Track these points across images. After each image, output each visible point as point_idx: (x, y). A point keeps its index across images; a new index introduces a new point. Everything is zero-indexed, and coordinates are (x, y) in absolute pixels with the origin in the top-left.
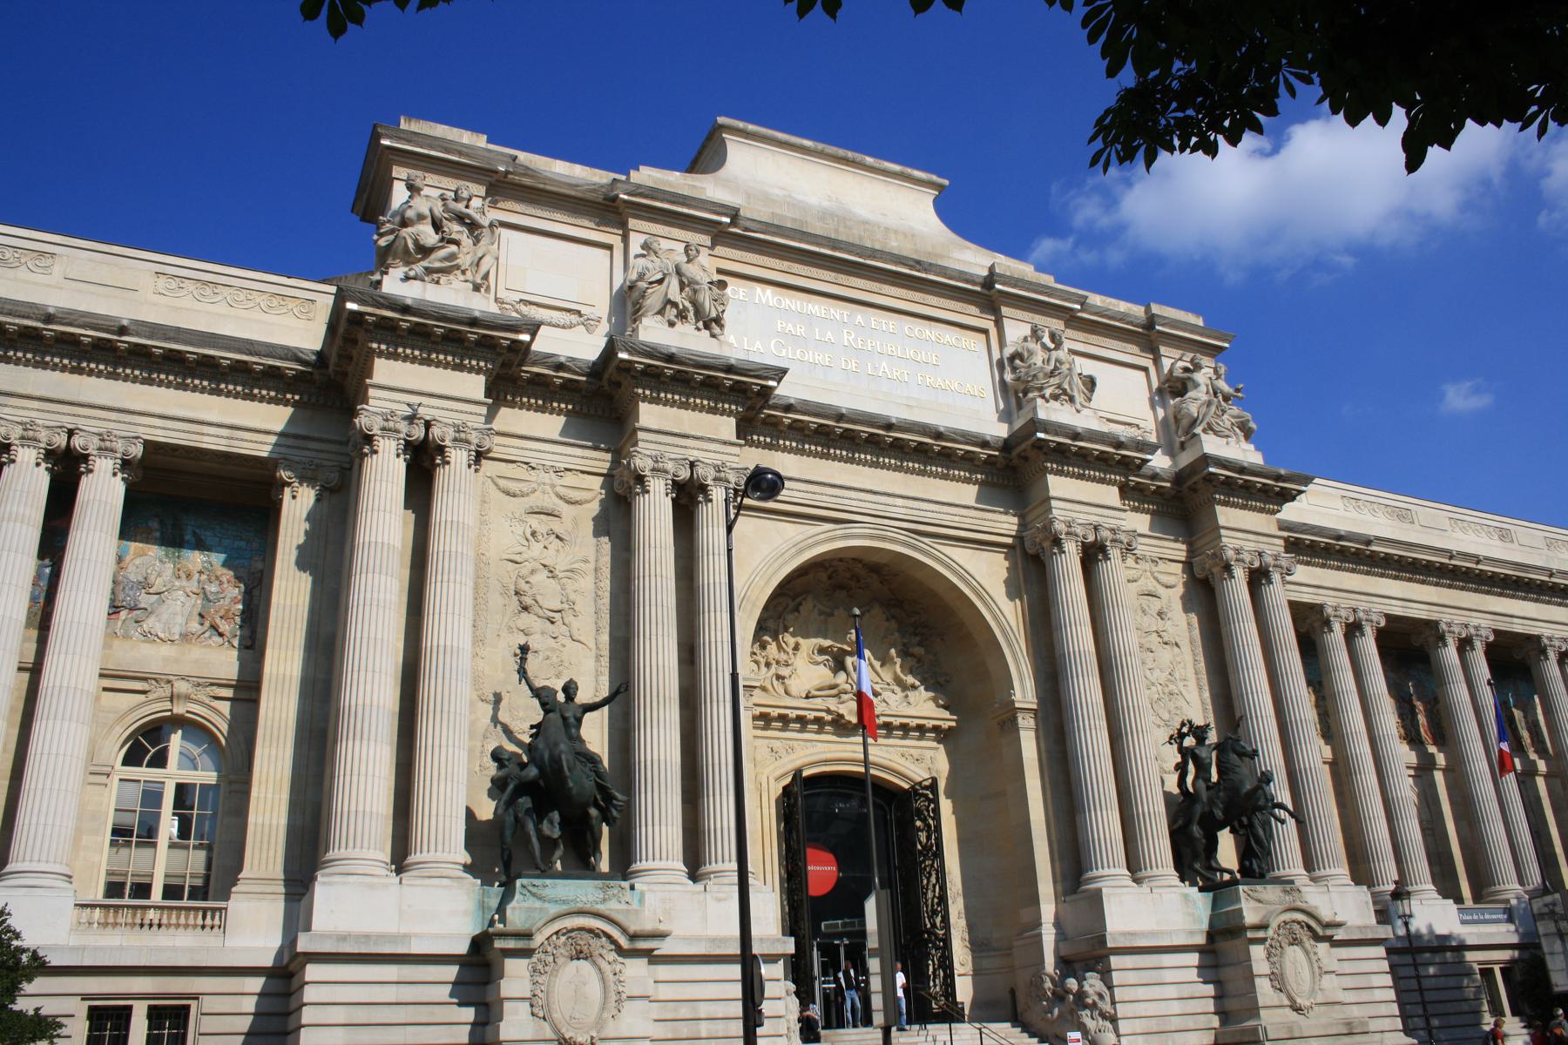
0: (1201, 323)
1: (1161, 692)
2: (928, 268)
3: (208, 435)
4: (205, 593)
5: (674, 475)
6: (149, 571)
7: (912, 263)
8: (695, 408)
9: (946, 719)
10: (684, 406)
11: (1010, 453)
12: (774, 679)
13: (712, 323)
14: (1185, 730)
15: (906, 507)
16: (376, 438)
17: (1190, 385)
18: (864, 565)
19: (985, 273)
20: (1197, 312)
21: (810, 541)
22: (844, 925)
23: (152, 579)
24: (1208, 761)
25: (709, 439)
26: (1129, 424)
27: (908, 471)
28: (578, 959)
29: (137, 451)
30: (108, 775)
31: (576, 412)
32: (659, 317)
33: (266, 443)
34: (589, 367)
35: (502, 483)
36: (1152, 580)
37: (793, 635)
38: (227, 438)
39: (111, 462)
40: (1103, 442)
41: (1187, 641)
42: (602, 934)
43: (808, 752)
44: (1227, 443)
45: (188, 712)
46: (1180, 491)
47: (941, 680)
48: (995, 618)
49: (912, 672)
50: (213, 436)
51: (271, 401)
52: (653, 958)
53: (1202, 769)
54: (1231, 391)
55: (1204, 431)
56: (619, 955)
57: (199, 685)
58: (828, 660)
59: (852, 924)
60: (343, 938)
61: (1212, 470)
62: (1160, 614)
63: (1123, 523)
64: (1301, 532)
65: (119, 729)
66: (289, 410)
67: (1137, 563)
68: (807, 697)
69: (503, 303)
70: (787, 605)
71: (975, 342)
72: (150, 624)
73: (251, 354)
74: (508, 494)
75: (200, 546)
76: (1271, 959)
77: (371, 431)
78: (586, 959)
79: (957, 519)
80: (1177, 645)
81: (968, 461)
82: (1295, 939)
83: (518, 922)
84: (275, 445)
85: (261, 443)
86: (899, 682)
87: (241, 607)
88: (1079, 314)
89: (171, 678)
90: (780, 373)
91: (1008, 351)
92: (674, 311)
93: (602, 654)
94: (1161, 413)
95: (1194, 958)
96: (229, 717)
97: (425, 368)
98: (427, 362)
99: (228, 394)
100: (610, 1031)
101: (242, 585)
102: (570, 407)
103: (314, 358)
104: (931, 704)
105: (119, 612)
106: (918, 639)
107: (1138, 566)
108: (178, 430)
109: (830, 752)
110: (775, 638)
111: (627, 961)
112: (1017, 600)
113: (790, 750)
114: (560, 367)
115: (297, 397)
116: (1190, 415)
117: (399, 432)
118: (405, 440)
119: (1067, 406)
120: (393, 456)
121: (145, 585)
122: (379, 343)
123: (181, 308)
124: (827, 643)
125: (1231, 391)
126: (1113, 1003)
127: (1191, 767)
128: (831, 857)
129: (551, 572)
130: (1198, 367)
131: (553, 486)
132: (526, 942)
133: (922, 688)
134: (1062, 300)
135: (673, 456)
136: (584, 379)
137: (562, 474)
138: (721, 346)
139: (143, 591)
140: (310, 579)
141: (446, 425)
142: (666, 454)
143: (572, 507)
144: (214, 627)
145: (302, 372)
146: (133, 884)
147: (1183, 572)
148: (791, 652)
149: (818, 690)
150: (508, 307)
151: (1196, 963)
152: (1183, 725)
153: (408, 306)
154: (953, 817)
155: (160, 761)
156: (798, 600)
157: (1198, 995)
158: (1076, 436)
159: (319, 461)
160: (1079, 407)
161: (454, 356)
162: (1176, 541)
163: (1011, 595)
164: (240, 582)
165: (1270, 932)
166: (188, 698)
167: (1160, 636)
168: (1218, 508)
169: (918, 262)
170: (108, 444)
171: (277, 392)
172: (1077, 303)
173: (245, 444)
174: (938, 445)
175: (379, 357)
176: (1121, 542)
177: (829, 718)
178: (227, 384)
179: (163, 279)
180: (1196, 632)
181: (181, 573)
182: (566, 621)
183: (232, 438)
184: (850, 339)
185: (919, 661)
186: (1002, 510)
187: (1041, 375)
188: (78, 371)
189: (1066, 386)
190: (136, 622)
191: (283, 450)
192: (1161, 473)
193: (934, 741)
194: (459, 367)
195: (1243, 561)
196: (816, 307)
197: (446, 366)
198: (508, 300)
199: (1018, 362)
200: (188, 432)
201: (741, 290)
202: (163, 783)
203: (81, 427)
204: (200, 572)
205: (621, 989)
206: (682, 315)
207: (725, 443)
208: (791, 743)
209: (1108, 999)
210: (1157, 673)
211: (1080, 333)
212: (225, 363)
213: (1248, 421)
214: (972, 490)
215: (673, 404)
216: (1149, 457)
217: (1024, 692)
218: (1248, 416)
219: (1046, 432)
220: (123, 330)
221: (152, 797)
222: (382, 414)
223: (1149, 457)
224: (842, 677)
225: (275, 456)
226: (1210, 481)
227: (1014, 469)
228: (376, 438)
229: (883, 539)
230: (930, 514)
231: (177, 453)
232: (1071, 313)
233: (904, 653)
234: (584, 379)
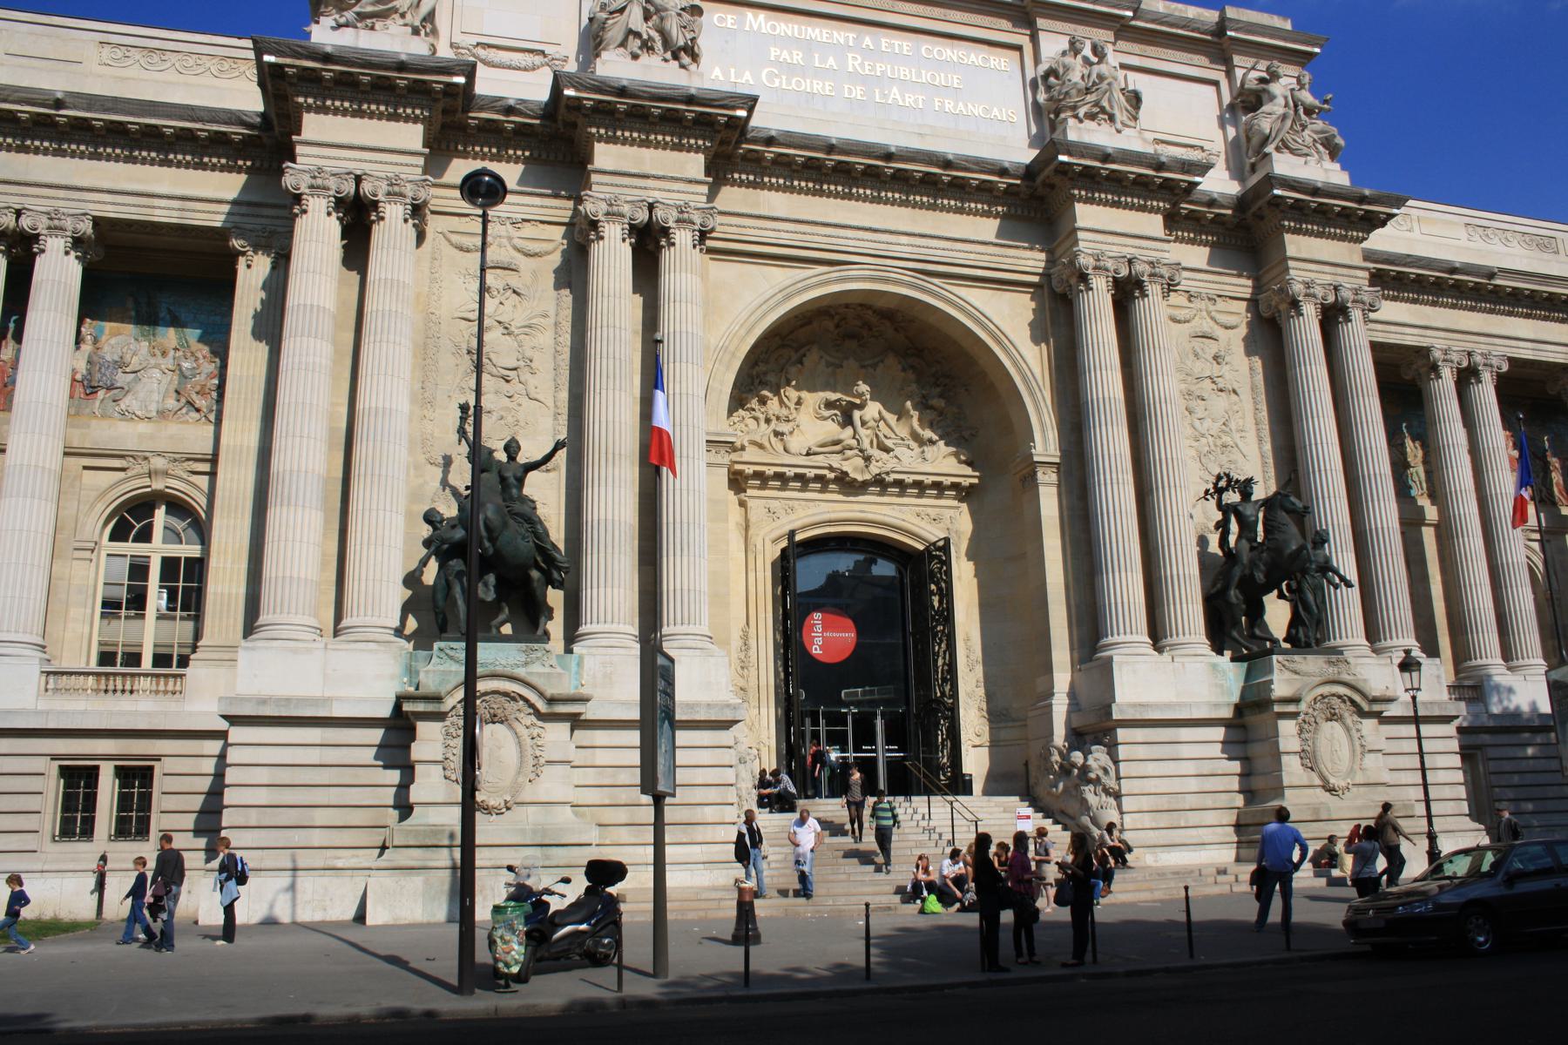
0: (1288, 25)
1: (1211, 444)
3: (160, 208)
4: (180, 370)
5: (631, 219)
6: (124, 350)
8: (657, 145)
9: (967, 476)
10: (645, 144)
11: (1034, 181)
12: (772, 435)
13: (687, 52)
14: (1222, 483)
15: (912, 245)
16: (304, 197)
17: (1265, 97)
18: (874, 312)
20: (1283, 14)
21: (799, 285)
22: (864, 693)
23: (127, 358)
24: (1253, 518)
25: (672, 178)
26: (1192, 147)
27: (915, 205)
28: (494, 723)
29: (86, 227)
30: (93, 551)
31: (535, 159)
32: (622, 49)
33: (218, 213)
34: (541, 109)
35: (455, 238)
36: (1209, 320)
37: (798, 388)
38: (179, 209)
39: (63, 241)
40: (1140, 164)
42: (517, 697)
43: (810, 512)
44: (1306, 163)
45: (167, 487)
46: (1245, 219)
47: (966, 434)
48: (1015, 364)
49: (932, 426)
50: (164, 208)
51: (223, 169)
52: (577, 722)
53: (1246, 527)
54: (1317, 103)
55: (1278, 149)
56: (539, 720)
57: (175, 460)
58: (836, 415)
59: (872, 692)
60: (263, 701)
61: (1277, 192)
62: (1216, 358)
63: (1166, 255)
64: (1405, 265)
65: (100, 506)
66: (243, 177)
67: (1190, 301)
68: (808, 454)
69: (458, 48)
70: (790, 359)
71: (1003, 62)
72: (128, 402)
73: (193, 120)
74: (461, 249)
75: (176, 322)
76: (1303, 736)
77: (299, 189)
78: (502, 722)
79: (972, 256)
80: (1235, 392)
81: (985, 192)
82: (1335, 714)
83: (431, 684)
84: (228, 214)
85: (214, 212)
86: (915, 436)
87: (217, 382)
88: (1133, 23)
89: (147, 454)
90: (751, 102)
91: (1043, 68)
92: (638, 42)
93: (560, 411)
94: (1231, 132)
95: (1219, 733)
96: (207, 491)
97: (357, 121)
98: (359, 114)
99: (179, 165)
100: (526, 796)
101: (217, 360)
102: (527, 154)
103: (259, 120)
104: (953, 460)
105: (96, 392)
106: (938, 390)
107: (1192, 305)
108: (129, 205)
109: (834, 512)
110: (777, 393)
111: (548, 725)
112: (1043, 345)
113: (789, 511)
114: (510, 110)
115: (249, 163)
116: (1261, 132)
117: (328, 189)
118: (335, 197)
119: (1106, 126)
120: (324, 215)
121: (121, 364)
122: (306, 97)
123: (127, 79)
124: (833, 396)
125: (1317, 103)
126: (1118, 778)
127: (1234, 527)
128: (849, 623)
129: (506, 328)
130: (1274, 76)
131: (510, 239)
132: (437, 705)
133: (942, 443)
135: (629, 198)
136: (538, 122)
137: (519, 225)
138: (690, 75)
139: (120, 370)
140: (267, 348)
141: (378, 178)
142: (623, 197)
143: (532, 259)
144: (190, 403)
145: (249, 135)
146: (124, 654)
147: (1248, 311)
148: (792, 406)
149: (822, 446)
150: (463, 51)
151: (1221, 739)
152: (1219, 478)
153: (328, 54)
154: (975, 581)
155: (145, 536)
156: (802, 351)
157: (1220, 772)
158: (1106, 157)
159: (273, 228)
160: (1119, 126)
161: (387, 105)
162: (1240, 276)
163: (1036, 340)
164: (216, 357)
165: (1303, 707)
166: (166, 474)
167: (1214, 382)
168: (1288, 237)
170: (56, 222)
171: (228, 158)
173: (198, 215)
174: (948, 175)
175: (308, 112)
176: (1162, 277)
177: (831, 475)
178: (176, 153)
179: (107, 49)
180: (1260, 379)
181: (156, 351)
182: (522, 379)
183: (183, 210)
184: (856, 63)
185: (941, 414)
186: (1026, 245)
187: (1074, 92)
188: (23, 149)
189: (1105, 103)
190: (114, 401)
191: (237, 219)
192: (1220, 199)
193: (955, 499)
194: (394, 117)
195: (1314, 296)
196: (817, 31)
197: (380, 116)
198: (463, 45)
199: (1052, 80)
200: (139, 206)
201: (729, 17)
202: (149, 557)
203: (27, 206)
204: (176, 349)
205: (538, 753)
206: (647, 46)
207: (690, 182)
208: (790, 503)
209: (1112, 773)
210: (1208, 423)
211: (1135, 45)
212: (169, 131)
213: (1334, 136)
214: (994, 224)
215: (633, 143)
216: (1197, 179)
217: (1046, 444)
218: (1334, 130)
219: (1070, 154)
221: (139, 570)
222: (309, 172)
223: (1197, 179)
224: (849, 431)
225: (228, 225)
226: (1277, 205)
227: (1041, 199)
228: (304, 197)
229: (886, 281)
231: (132, 229)
232: (1122, 21)
233: (923, 405)
234: (538, 122)
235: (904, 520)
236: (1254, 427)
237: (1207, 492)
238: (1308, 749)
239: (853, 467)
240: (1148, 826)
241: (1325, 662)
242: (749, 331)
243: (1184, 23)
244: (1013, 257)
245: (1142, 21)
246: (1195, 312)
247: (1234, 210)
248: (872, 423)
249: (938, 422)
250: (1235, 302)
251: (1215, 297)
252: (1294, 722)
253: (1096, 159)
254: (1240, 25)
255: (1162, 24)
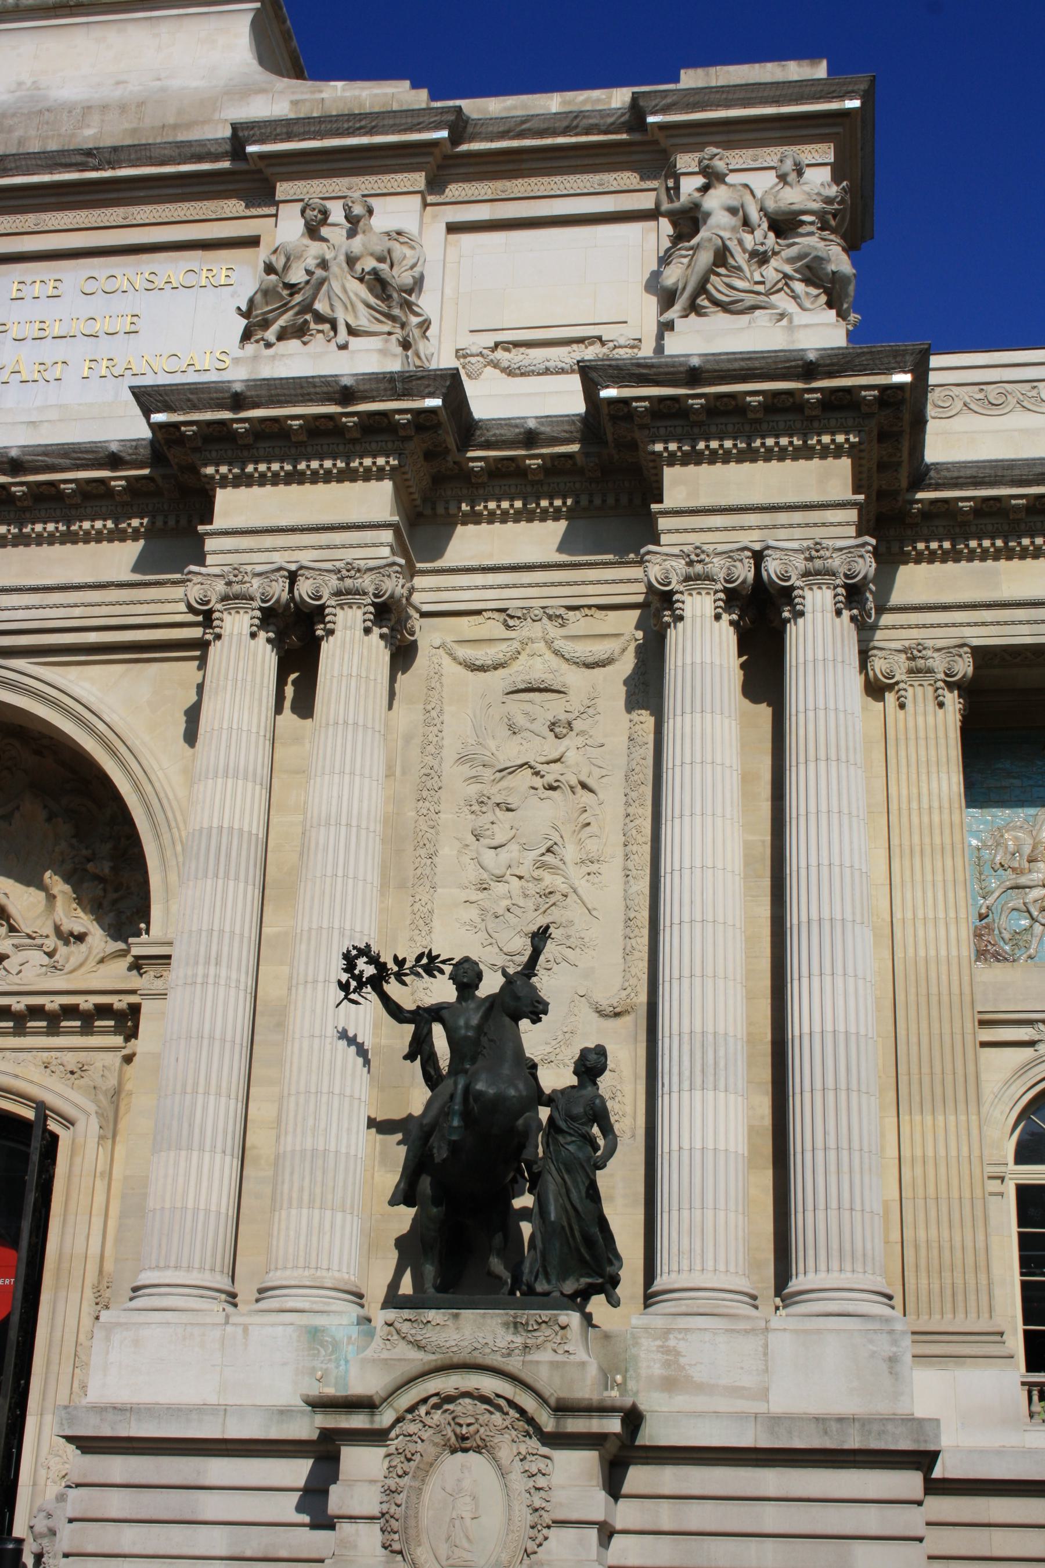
2: (113, 157)
7: (79, 159)
19: (228, 133)
36: (549, 656)
41: (620, 775)
62: (552, 726)
67: (508, 627)
79: (77, 612)
80: (584, 786)
88: (464, 147)
134: (400, 132)
151: (301, 1483)
157: (284, 1553)
160: (343, 334)
165: (385, 1418)
167: (537, 773)
169: (89, 153)
172: (437, 127)
189: (320, 306)
192: (543, 429)
195: (709, 578)
214: (133, 549)
219: (167, 408)
232: (436, 151)
235: (16, 1076)
236: (620, 851)
237: (344, 987)
238: (393, 1509)
241: (506, 1325)
243: (565, 124)
244: (153, 602)
245: (482, 140)
246: (516, 645)
247: (582, 441)
249: (114, 902)
250: (612, 614)
251: (562, 611)
252: (382, 1451)
253: (221, 406)
254: (669, 100)
255: (521, 135)
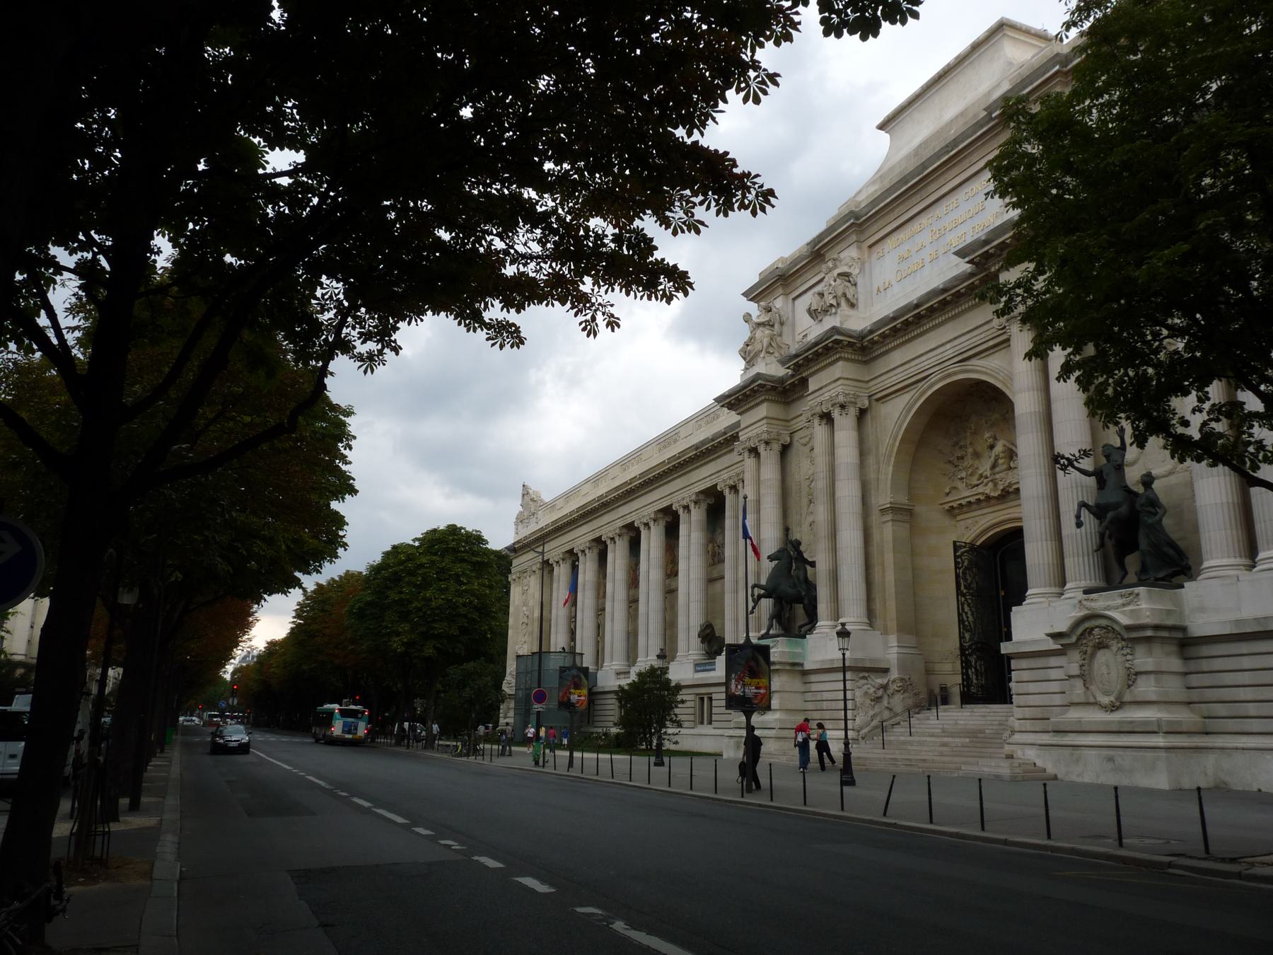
172: (1054, 66)
208: (974, 519)
220: (725, 433)
230: (965, 344)
239: (988, 489)
240: (1029, 730)
242: (895, 440)
248: (1001, 455)
